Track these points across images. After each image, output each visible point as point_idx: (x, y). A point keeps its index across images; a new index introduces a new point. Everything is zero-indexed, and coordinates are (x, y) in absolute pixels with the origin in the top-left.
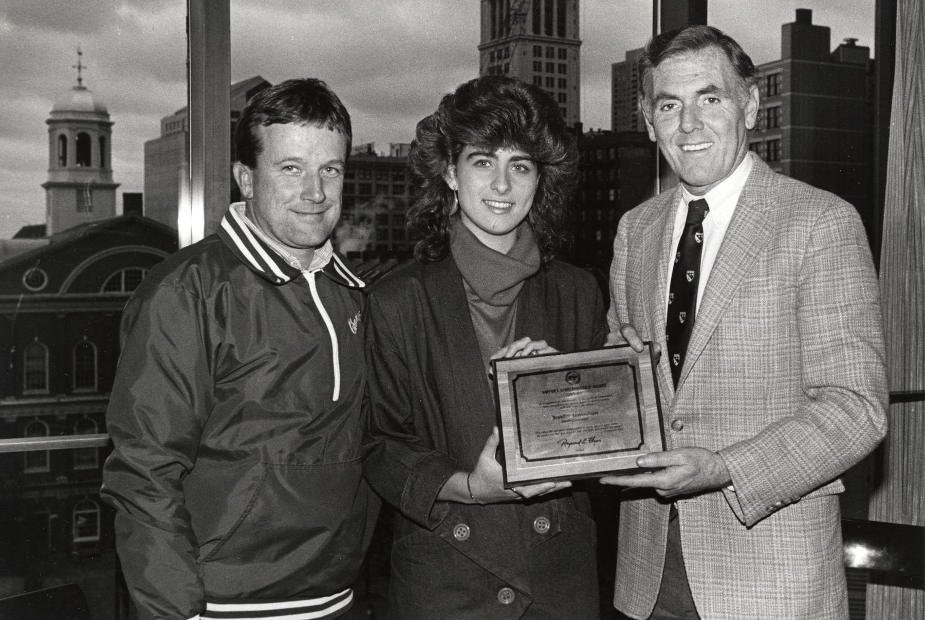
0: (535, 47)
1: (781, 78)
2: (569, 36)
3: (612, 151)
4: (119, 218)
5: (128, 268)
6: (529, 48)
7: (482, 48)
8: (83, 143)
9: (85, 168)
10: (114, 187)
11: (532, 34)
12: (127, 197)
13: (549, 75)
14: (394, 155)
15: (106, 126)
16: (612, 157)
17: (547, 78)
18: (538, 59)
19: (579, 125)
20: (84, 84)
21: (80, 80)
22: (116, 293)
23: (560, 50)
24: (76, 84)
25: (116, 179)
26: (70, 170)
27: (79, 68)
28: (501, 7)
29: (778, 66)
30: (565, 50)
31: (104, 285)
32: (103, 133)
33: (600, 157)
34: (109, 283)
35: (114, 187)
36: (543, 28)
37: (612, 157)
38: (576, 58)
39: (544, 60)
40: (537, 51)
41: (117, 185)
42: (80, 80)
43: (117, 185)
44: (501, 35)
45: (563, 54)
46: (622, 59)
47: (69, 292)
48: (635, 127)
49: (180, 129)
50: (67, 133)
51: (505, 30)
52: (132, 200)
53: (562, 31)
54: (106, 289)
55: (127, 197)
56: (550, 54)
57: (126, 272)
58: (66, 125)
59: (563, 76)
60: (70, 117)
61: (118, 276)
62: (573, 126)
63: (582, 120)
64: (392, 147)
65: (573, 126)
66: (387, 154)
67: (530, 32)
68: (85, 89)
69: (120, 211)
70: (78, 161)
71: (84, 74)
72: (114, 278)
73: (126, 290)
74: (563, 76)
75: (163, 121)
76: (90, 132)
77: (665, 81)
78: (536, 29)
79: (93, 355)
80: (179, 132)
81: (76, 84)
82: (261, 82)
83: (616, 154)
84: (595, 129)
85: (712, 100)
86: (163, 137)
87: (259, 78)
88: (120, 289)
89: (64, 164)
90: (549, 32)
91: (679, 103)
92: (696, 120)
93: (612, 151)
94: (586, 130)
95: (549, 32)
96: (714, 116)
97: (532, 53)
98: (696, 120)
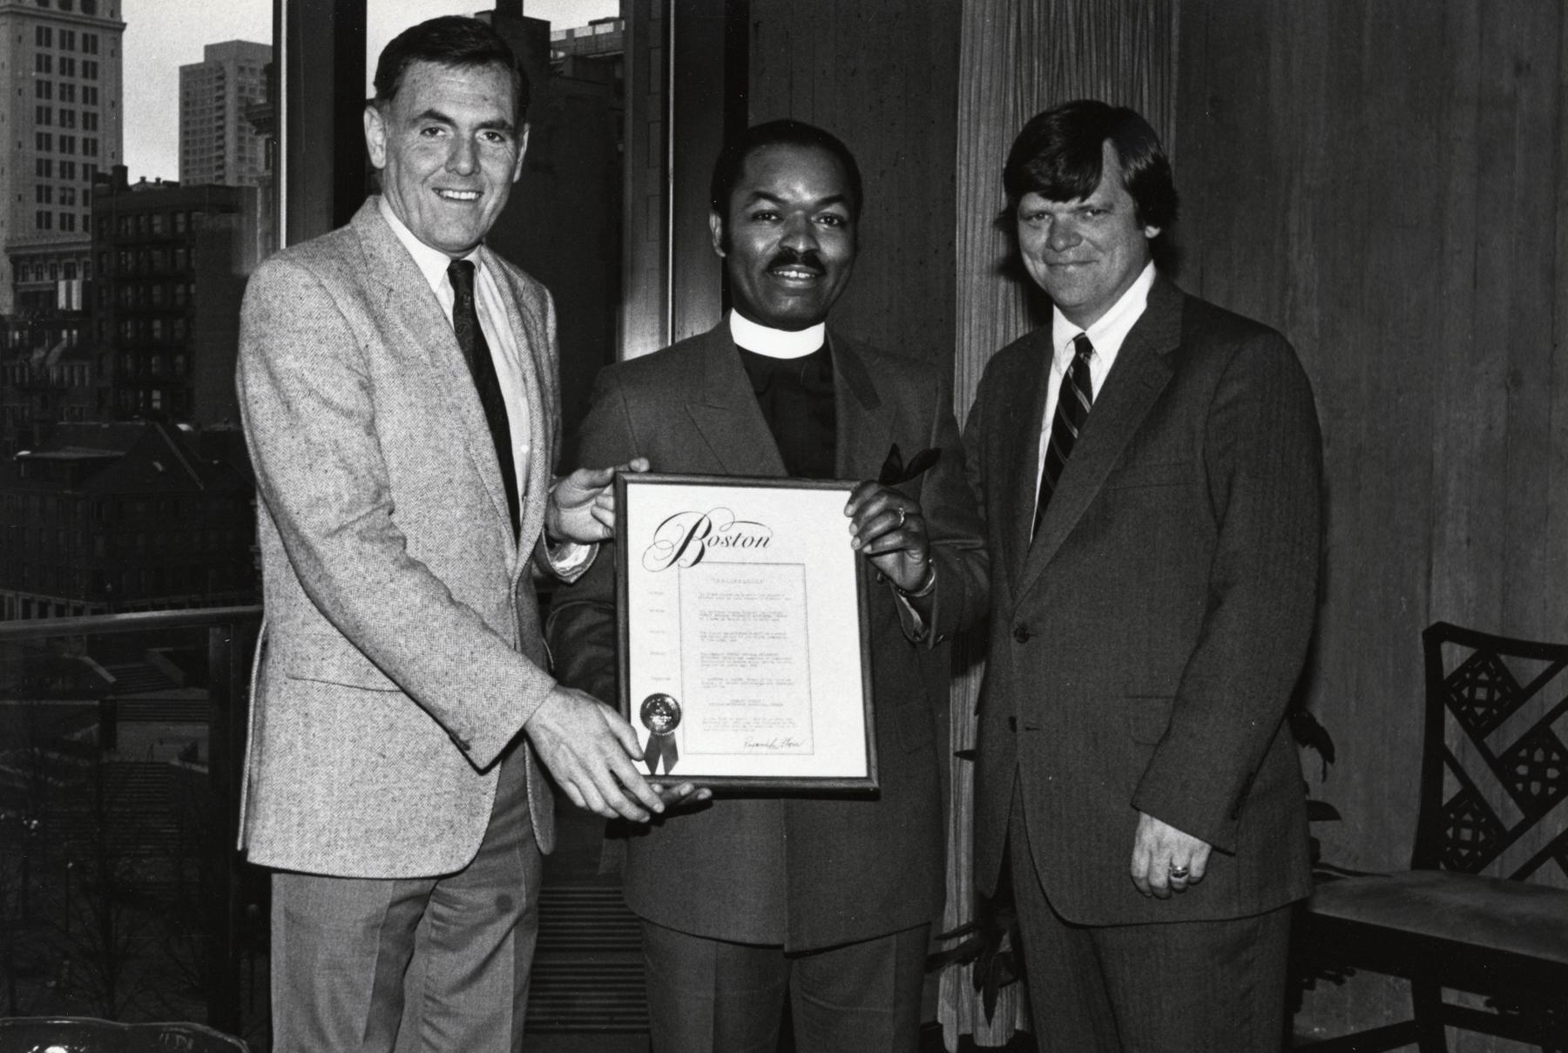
0: (39, 29)
2: (102, 13)
3: (181, 218)
6: (30, 29)
13: (65, 79)
16: (181, 228)
17: (63, 85)
19: (122, 171)
23: (85, 36)
30: (95, 38)
33: (157, 229)
37: (181, 228)
38: (116, 53)
40: (43, 37)
45: (90, 44)
46: (199, 58)
48: (221, 177)
56: (67, 41)
59: (90, 83)
62: (110, 172)
63: (126, 162)
65: (110, 172)
74: (90, 83)
83: (189, 222)
84: (151, 179)
91: (451, 133)
93: (181, 218)
94: (133, 179)
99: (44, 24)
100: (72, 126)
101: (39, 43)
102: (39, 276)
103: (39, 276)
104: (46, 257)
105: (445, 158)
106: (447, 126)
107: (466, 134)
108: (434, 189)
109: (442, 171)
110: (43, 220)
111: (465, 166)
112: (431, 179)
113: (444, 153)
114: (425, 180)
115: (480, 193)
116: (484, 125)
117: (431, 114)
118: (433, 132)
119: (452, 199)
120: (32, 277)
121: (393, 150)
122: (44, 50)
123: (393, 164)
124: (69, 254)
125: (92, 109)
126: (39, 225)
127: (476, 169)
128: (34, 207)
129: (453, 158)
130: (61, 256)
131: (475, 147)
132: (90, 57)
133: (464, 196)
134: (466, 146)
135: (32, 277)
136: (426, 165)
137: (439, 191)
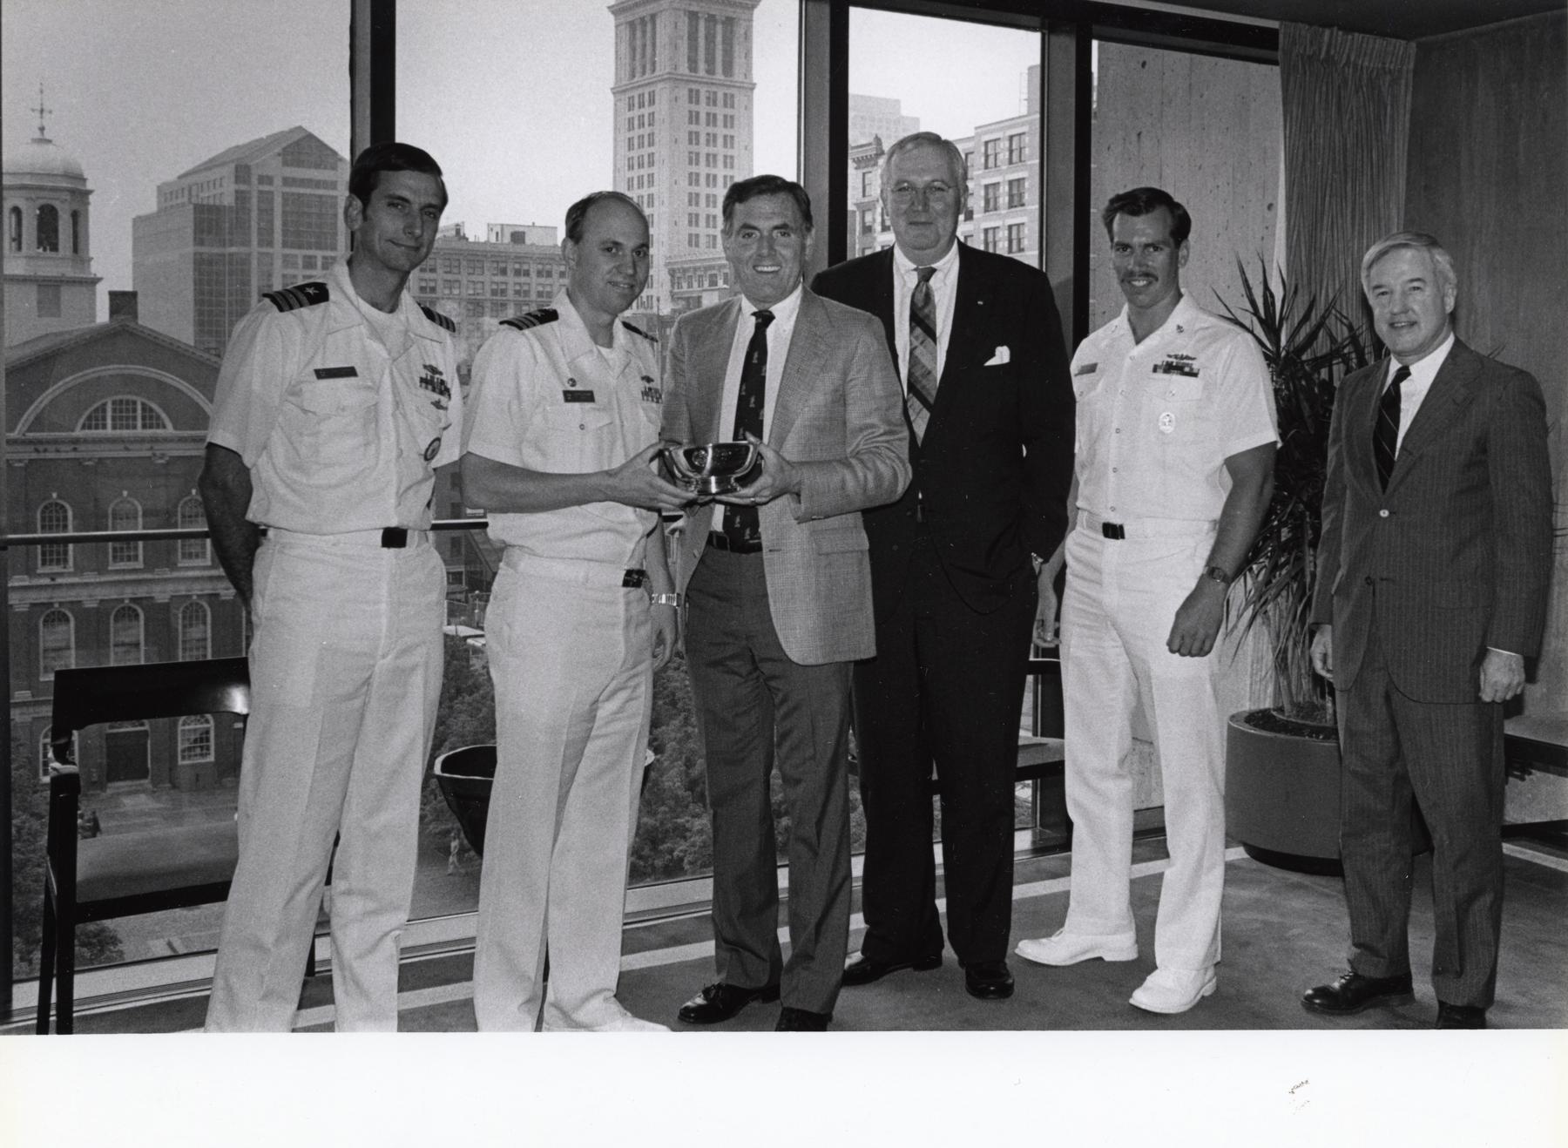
0: (691, 91)
1: (1027, 139)
2: (738, 76)
4: (103, 327)
5: (118, 397)
6: (683, 93)
7: (617, 92)
8: (47, 219)
9: (53, 254)
10: (95, 281)
11: (687, 72)
12: (114, 295)
14: (493, 240)
15: (81, 195)
18: (694, 107)
20: (47, 135)
21: (42, 129)
22: (100, 433)
24: (38, 135)
25: (96, 269)
26: (30, 258)
27: (42, 111)
28: (644, 32)
29: (1023, 124)
31: (81, 421)
32: (75, 206)
34: (89, 418)
35: (95, 281)
36: (702, 66)
38: (749, 108)
39: (703, 109)
40: (694, 97)
41: (100, 279)
42: (42, 129)
43: (100, 279)
44: (644, 73)
45: (729, 101)
47: (29, 430)
49: (186, 199)
50: (22, 204)
51: (648, 66)
52: (123, 302)
53: (728, 68)
54: (83, 427)
55: (114, 295)
56: (712, 100)
57: (114, 403)
58: (24, 193)
60: (27, 181)
61: (103, 408)
64: (490, 228)
66: (483, 239)
67: (684, 69)
68: (49, 141)
69: (103, 315)
70: (40, 243)
71: (47, 121)
72: (96, 410)
73: (114, 427)
75: (159, 188)
76: (57, 204)
77: (749, 214)
78: (693, 64)
79: (65, 518)
80: (183, 205)
81: (38, 135)
82: (302, 135)
85: (783, 234)
86: (159, 211)
87: (300, 128)
88: (104, 427)
89: (19, 248)
90: (711, 71)
92: (771, 248)
95: (711, 71)
96: (785, 246)
97: (686, 98)
98: (771, 248)
99: (694, 87)
100: (715, 166)
101: (691, 102)
102: (690, 285)
103: (690, 285)
104: (695, 269)
110: (693, 240)
111: (765, 251)
117: (746, 226)
120: (685, 285)
122: (694, 107)
124: (713, 267)
125: (730, 152)
126: (690, 244)
128: (685, 230)
129: (759, 248)
130: (707, 269)
132: (729, 111)
135: (685, 285)
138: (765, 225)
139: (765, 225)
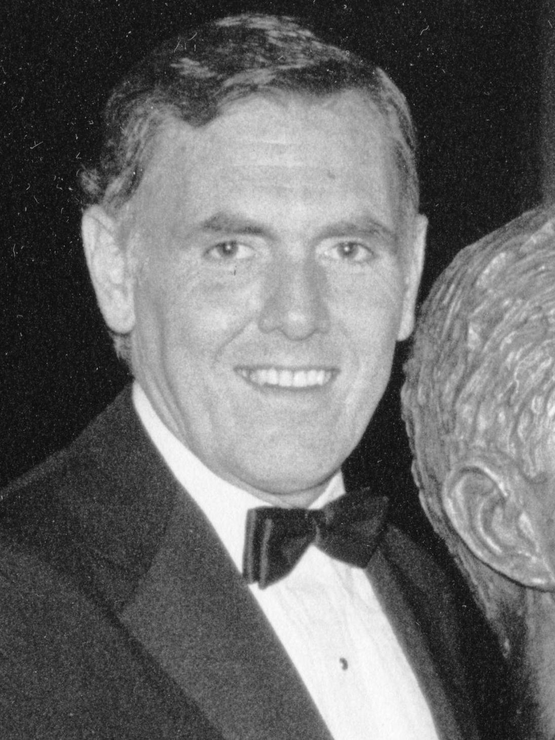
105: (256, 304)
106: (259, 240)
107: (296, 251)
108: (237, 369)
109: (253, 327)
111: (297, 318)
112: (229, 350)
113: (251, 296)
114: (220, 351)
115: (334, 372)
116: (332, 232)
118: (227, 250)
119: (276, 389)
121: (150, 296)
123: (150, 321)
127: (320, 326)
129: (274, 302)
131: (316, 277)
133: (301, 380)
134: (298, 277)
136: (215, 320)
137: (247, 371)
138: (295, 217)
139: (295, 217)
